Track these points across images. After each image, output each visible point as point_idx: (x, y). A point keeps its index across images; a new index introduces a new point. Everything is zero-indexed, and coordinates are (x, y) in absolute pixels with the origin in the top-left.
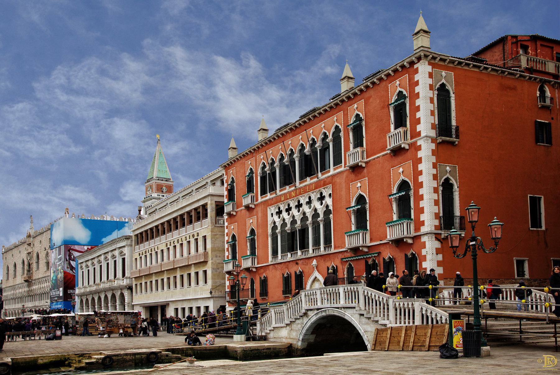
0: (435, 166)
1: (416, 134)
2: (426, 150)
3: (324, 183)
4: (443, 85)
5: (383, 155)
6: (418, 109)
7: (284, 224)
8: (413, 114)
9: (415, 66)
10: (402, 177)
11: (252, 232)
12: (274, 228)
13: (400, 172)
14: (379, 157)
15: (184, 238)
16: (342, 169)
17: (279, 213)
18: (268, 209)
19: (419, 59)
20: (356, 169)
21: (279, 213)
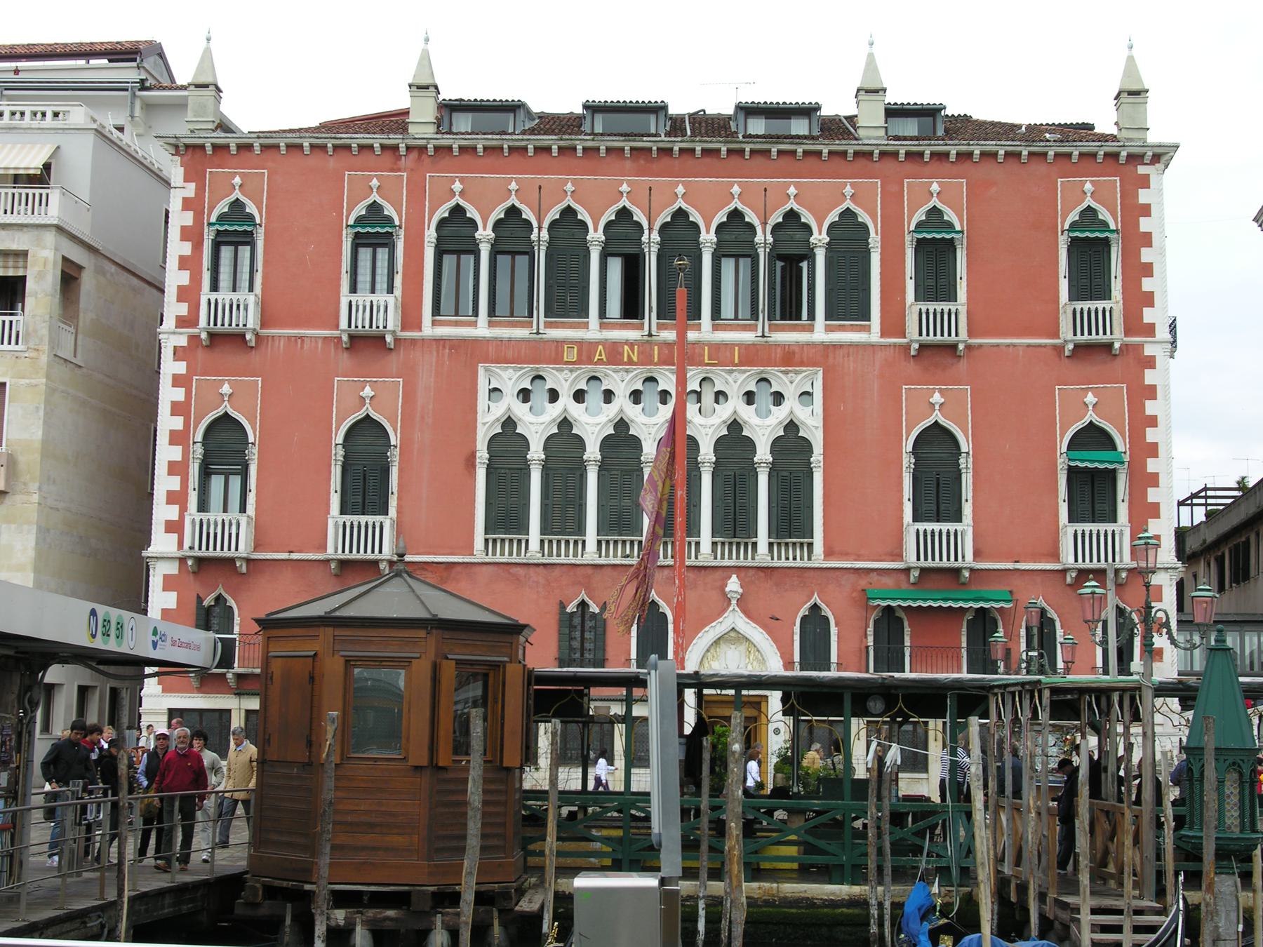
5: (1029, 346)
9: (1142, 170)
10: (1091, 416)
12: (509, 439)
14: (1014, 345)
18: (481, 371)
20: (937, 355)
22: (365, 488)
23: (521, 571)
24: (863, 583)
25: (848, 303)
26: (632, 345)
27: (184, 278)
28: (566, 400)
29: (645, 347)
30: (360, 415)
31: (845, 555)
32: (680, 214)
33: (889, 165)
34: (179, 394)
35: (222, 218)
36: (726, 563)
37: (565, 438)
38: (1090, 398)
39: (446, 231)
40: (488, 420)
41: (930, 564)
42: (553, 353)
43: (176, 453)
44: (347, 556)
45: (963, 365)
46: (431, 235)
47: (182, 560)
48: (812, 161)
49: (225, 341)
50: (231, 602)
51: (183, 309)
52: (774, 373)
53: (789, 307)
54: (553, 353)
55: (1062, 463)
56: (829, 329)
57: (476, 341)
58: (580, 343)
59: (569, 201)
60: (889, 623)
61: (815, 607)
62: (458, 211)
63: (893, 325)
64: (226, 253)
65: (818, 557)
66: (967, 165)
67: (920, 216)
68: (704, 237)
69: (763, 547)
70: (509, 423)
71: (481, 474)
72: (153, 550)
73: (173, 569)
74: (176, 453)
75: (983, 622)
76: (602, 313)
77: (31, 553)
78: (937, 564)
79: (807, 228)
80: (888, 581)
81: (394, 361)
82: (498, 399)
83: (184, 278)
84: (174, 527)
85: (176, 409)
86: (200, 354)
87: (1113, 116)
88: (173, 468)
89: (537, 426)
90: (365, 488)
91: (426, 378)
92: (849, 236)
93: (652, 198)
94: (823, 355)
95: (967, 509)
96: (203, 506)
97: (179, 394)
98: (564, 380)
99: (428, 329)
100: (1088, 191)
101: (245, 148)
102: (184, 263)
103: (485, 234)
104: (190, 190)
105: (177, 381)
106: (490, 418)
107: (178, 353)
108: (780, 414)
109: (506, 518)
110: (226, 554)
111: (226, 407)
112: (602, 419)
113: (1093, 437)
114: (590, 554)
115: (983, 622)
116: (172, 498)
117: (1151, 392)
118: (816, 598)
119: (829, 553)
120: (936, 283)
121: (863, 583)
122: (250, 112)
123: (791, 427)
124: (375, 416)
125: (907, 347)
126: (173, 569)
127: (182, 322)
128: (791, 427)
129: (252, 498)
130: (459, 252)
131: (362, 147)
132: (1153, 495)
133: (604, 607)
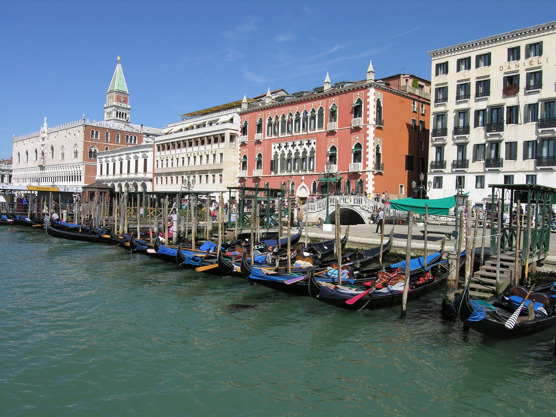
0: (374, 139)
1: (366, 122)
2: (371, 130)
3: (312, 136)
4: (379, 99)
6: (368, 110)
7: (283, 154)
8: (365, 113)
11: (260, 155)
12: (276, 155)
13: (356, 138)
15: (203, 153)
16: (324, 130)
17: (279, 147)
19: (370, 86)
21: (279, 147)
25: (320, 126)
65: (315, 173)
89: (279, 153)
91: (266, 146)
128: (313, 148)
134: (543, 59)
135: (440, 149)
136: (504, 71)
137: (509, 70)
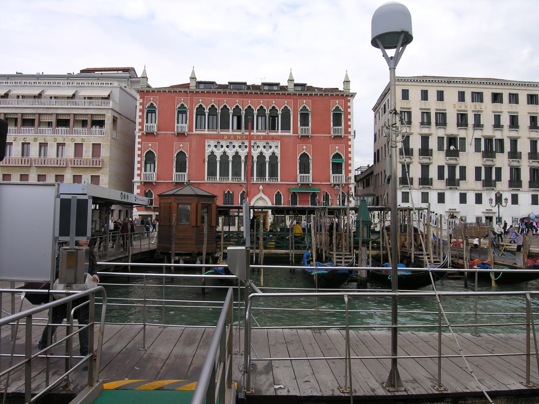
9: (349, 98)
10: (337, 151)
16: (291, 133)
20: (305, 138)
22: (181, 167)
23: (215, 185)
24: (288, 187)
25: (286, 127)
26: (239, 135)
27: (140, 120)
28: (225, 147)
29: (242, 136)
30: (180, 151)
31: (285, 181)
32: (249, 107)
33: (295, 96)
34: (140, 146)
35: (148, 107)
36: (259, 182)
37: (224, 156)
38: (337, 147)
39: (198, 110)
40: (208, 151)
41: (303, 183)
42: (222, 137)
43: (139, 159)
44: (177, 181)
45: (310, 140)
46: (195, 111)
47: (141, 182)
48: (278, 95)
49: (150, 134)
50: (152, 191)
51: (140, 127)
52: (269, 141)
53: (273, 127)
54: (222, 137)
55: (331, 161)
56: (281, 132)
57: (205, 134)
58: (228, 135)
59: (225, 104)
60: (294, 195)
61: (278, 192)
62: (201, 106)
63: (295, 131)
64: (150, 115)
66: (311, 97)
67: (301, 108)
68: (254, 112)
69: (267, 179)
70: (212, 152)
71: (206, 163)
72: (135, 180)
73: (139, 184)
74: (139, 159)
75: (314, 195)
76: (233, 129)
77: (108, 181)
78: (304, 183)
79: (277, 110)
80: (294, 186)
81: (187, 139)
82: (210, 147)
83: (140, 120)
84: (139, 175)
85: (139, 149)
86: (144, 137)
87: (343, 86)
88: (139, 162)
89: (218, 153)
90: (181, 167)
92: (286, 112)
93: (243, 104)
94: (280, 138)
95: (311, 171)
96: (145, 171)
97: (140, 146)
98: (224, 143)
99: (194, 132)
100: (338, 103)
101: (153, 91)
102: (140, 117)
103: (207, 111)
104: (141, 101)
105: (139, 143)
106: (208, 151)
107: (139, 137)
108: (271, 151)
109: (212, 173)
110: (151, 181)
111: (150, 149)
112: (233, 151)
113: (337, 156)
114: (230, 181)
115: (314, 195)
116: (139, 169)
117: (350, 146)
118: (278, 190)
119: (281, 181)
120: (305, 123)
121: (288, 187)
122: (155, 83)
123: (273, 153)
124: (183, 151)
125: (298, 136)
126: (139, 184)
127: (140, 130)
128: (273, 153)
129: (156, 169)
130: (201, 115)
131: (179, 91)
132: (350, 168)
133: (233, 192)
134: (483, 105)
135: (406, 168)
136: (457, 108)
137: (460, 109)
